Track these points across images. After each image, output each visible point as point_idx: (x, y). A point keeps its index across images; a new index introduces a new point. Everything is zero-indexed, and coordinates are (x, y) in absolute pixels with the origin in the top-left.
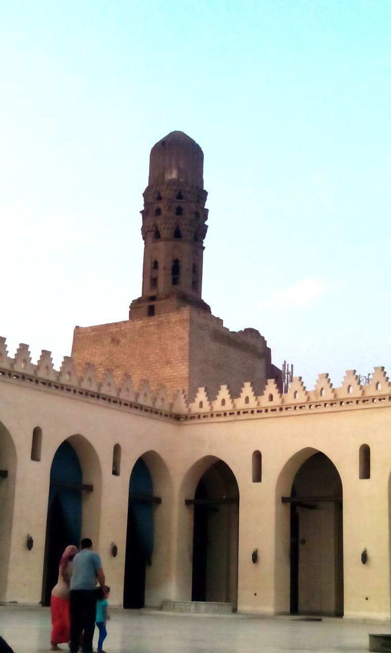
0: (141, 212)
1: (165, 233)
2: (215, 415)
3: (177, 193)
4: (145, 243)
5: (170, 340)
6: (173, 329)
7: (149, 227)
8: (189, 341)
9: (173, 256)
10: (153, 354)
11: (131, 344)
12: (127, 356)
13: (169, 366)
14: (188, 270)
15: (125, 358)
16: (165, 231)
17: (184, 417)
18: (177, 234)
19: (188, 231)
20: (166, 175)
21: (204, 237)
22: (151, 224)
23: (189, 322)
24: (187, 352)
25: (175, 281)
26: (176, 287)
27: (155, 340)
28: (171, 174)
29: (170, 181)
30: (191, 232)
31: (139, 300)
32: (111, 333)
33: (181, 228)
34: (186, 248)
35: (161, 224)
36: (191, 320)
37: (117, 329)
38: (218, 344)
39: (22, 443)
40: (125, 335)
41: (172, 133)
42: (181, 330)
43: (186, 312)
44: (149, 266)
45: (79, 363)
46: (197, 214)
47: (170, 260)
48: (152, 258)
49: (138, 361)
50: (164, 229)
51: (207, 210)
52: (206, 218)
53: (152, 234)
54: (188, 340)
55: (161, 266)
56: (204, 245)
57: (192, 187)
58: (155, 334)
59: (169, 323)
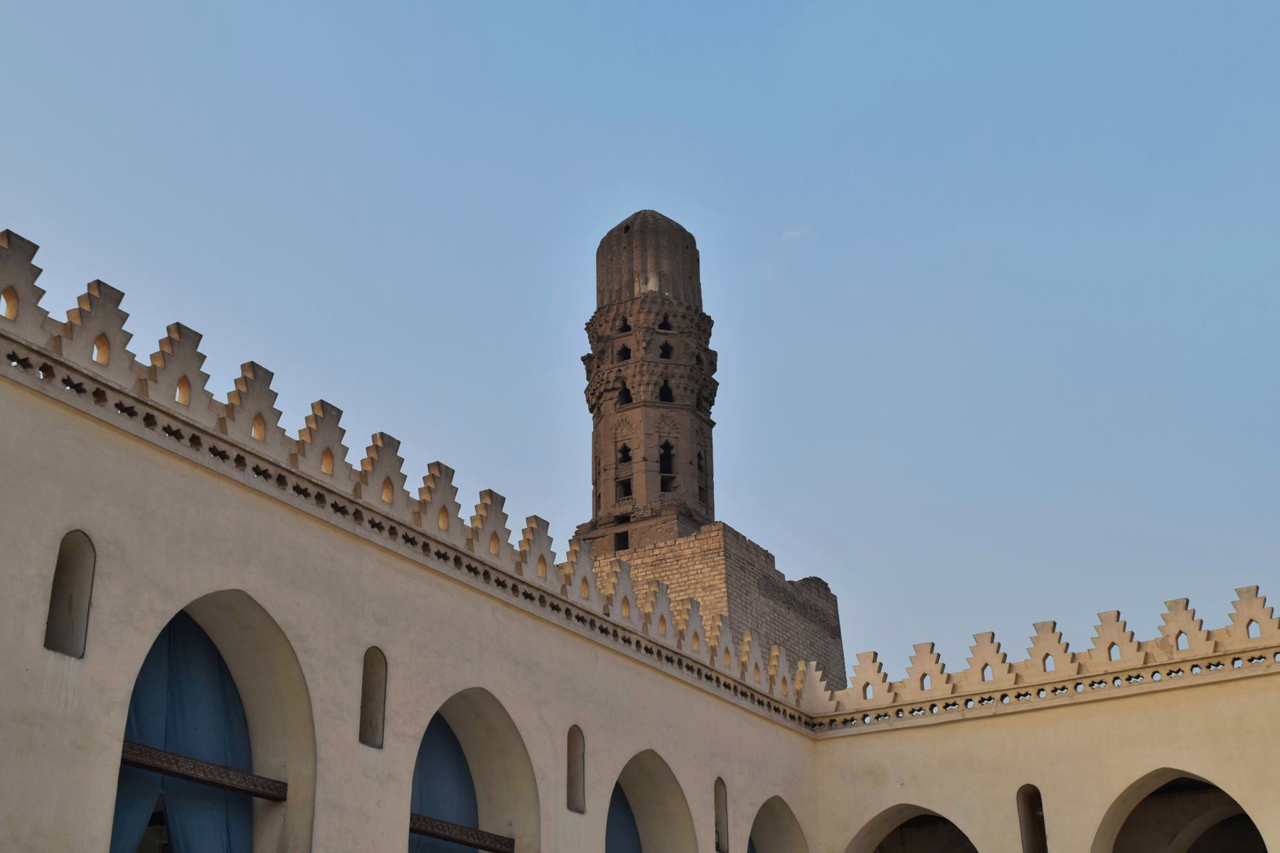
0: (583, 359)
1: (641, 393)
2: (907, 710)
3: (661, 318)
5: (681, 594)
6: (689, 571)
7: (608, 382)
8: (727, 592)
14: (691, 463)
16: (642, 388)
17: (826, 721)
18: (665, 394)
19: (685, 389)
20: (636, 285)
21: (712, 403)
23: (721, 554)
25: (666, 485)
26: (669, 495)
29: (646, 295)
30: (692, 391)
31: (593, 525)
33: (672, 383)
35: (634, 376)
38: (771, 603)
41: (637, 214)
44: (611, 457)
46: (699, 359)
47: (655, 442)
50: (640, 385)
51: (715, 354)
52: (715, 370)
53: (616, 394)
54: (725, 590)
55: (637, 454)
56: (712, 417)
57: (689, 308)
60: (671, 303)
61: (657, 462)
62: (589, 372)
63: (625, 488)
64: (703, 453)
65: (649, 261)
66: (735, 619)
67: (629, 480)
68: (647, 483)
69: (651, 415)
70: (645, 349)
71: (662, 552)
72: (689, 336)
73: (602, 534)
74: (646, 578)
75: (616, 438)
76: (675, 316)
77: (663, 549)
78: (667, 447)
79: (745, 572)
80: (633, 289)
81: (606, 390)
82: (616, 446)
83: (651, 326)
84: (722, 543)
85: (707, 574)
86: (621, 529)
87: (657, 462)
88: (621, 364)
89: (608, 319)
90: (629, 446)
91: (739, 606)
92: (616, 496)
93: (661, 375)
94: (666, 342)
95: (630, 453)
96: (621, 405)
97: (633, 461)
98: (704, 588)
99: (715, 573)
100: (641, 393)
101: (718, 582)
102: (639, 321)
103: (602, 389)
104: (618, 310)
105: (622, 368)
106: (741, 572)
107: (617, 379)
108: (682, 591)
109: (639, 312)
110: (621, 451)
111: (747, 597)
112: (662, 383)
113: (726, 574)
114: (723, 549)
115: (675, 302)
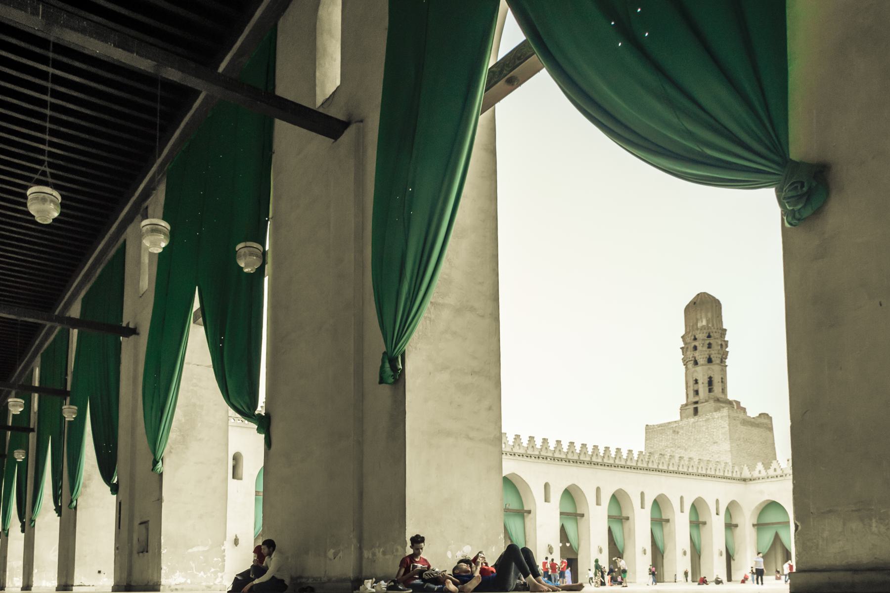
1: (701, 361)
2: (770, 477)
3: (707, 334)
4: (686, 368)
16: (701, 360)
18: (710, 361)
25: (710, 391)
26: (711, 394)
28: (702, 322)
30: (719, 358)
31: (686, 405)
32: (672, 427)
33: (712, 356)
34: (715, 368)
35: (698, 356)
36: (729, 416)
39: (636, 501)
40: (682, 428)
42: (722, 422)
43: (725, 411)
44: (691, 383)
45: (651, 447)
48: (693, 378)
53: (692, 362)
55: (700, 382)
57: (718, 329)
58: (703, 426)
59: (713, 418)
60: (711, 329)
62: (683, 352)
63: (697, 392)
76: (712, 332)
77: (709, 416)
78: (710, 378)
86: (695, 406)
90: (697, 378)
93: (708, 354)
95: (698, 381)
98: (722, 428)
100: (701, 361)
103: (687, 360)
107: (693, 357)
109: (700, 333)
112: (708, 356)
115: (712, 328)
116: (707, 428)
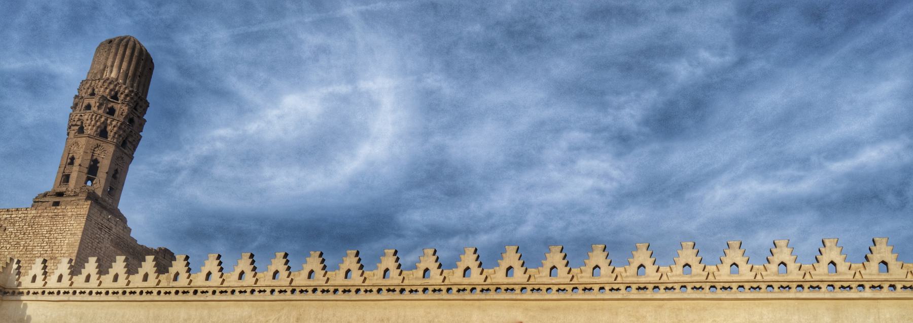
1: (89, 130)
5: (60, 235)
8: (82, 238)
9: (93, 155)
10: (38, 247)
11: (19, 234)
12: (10, 246)
13: (53, 261)
15: (8, 248)
16: (90, 127)
18: (103, 133)
22: (77, 117)
23: (85, 217)
24: (76, 249)
27: (45, 233)
28: (111, 72)
29: (108, 79)
33: (109, 128)
35: (87, 120)
36: (88, 216)
37: (9, 216)
49: (21, 253)
50: (89, 125)
53: (77, 128)
54: (80, 236)
55: (77, 162)
61: (87, 168)
63: (66, 178)
64: (119, 170)
65: (116, 61)
66: (82, 253)
67: (70, 175)
68: (77, 178)
69: (91, 143)
70: (99, 108)
71: (59, 211)
72: (126, 106)
73: (47, 200)
74: (46, 223)
75: (70, 151)
79: (101, 231)
80: (103, 74)
81: (72, 125)
82: (68, 156)
83: (105, 95)
84: (87, 212)
85: (74, 227)
87: (87, 168)
88: (84, 112)
89: (85, 87)
90: (75, 157)
91: (89, 247)
92: (61, 182)
94: (113, 106)
96: (78, 134)
97: (75, 165)
98: (71, 234)
99: (78, 227)
101: (78, 232)
102: (100, 91)
104: (91, 83)
105: (82, 114)
106: (98, 230)
107: (79, 120)
108: (61, 233)
109: (101, 87)
110: (70, 159)
111: (98, 245)
112: (103, 126)
113: (84, 228)
114: (86, 215)
116: (50, 232)
